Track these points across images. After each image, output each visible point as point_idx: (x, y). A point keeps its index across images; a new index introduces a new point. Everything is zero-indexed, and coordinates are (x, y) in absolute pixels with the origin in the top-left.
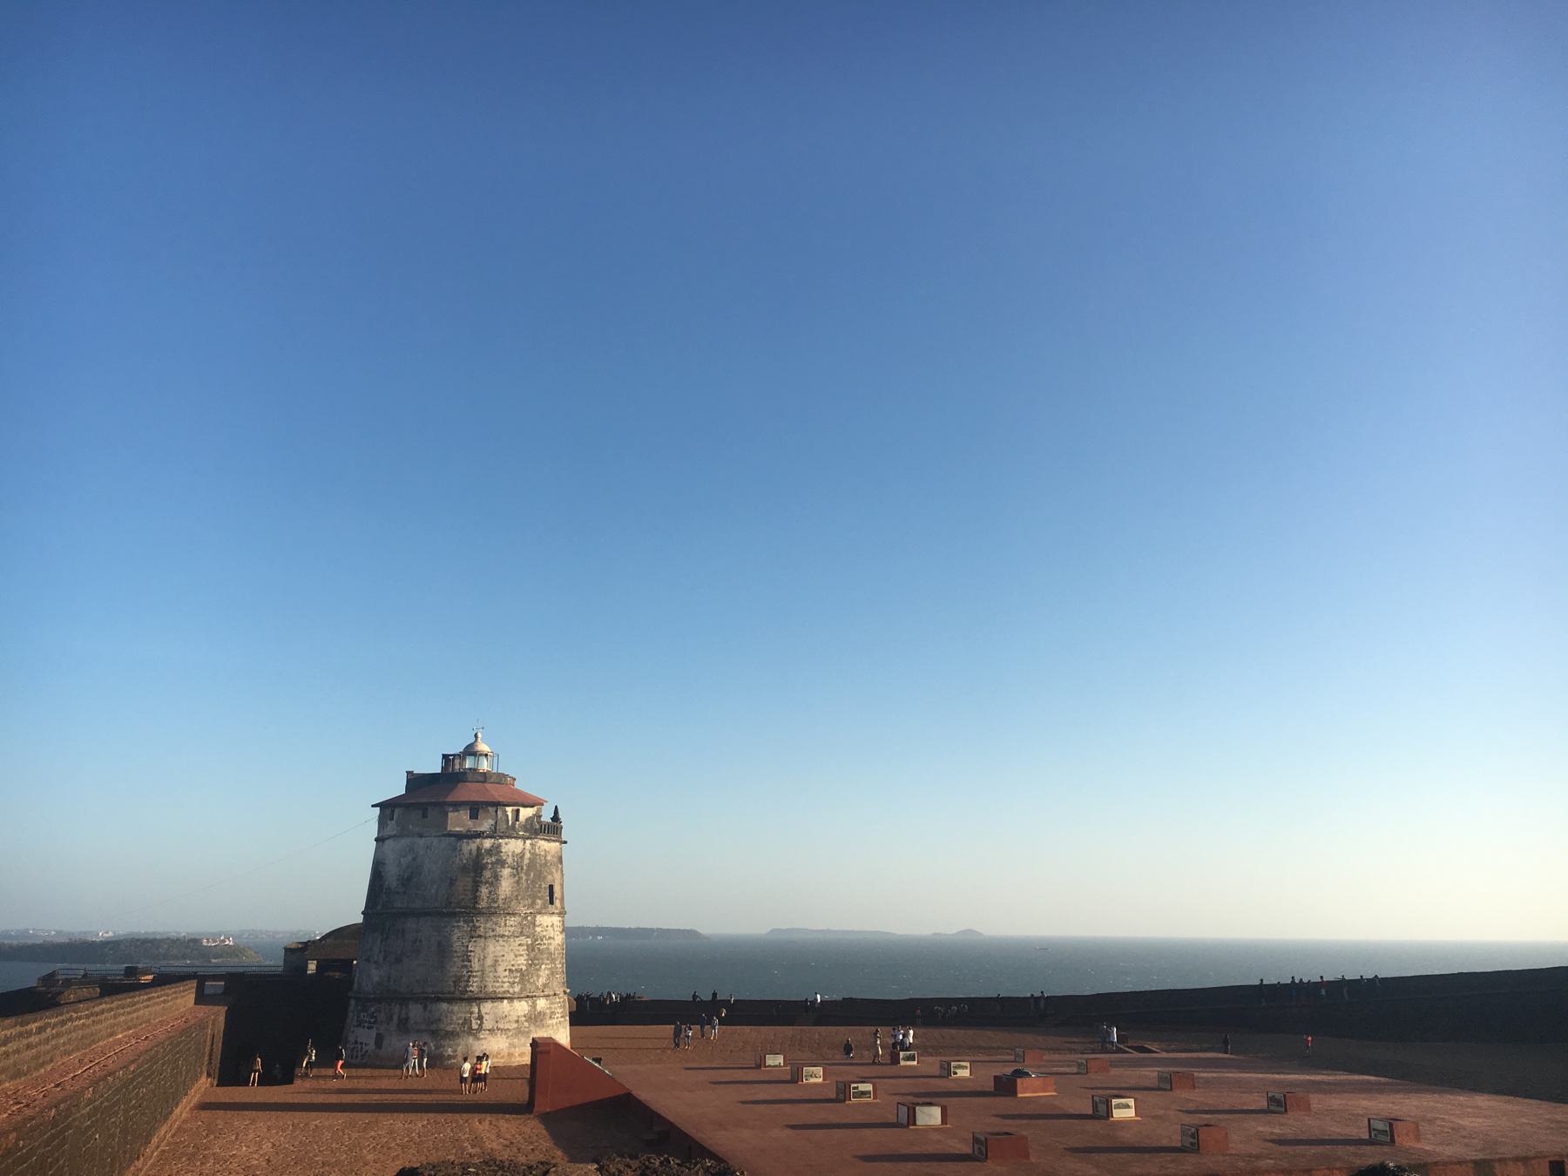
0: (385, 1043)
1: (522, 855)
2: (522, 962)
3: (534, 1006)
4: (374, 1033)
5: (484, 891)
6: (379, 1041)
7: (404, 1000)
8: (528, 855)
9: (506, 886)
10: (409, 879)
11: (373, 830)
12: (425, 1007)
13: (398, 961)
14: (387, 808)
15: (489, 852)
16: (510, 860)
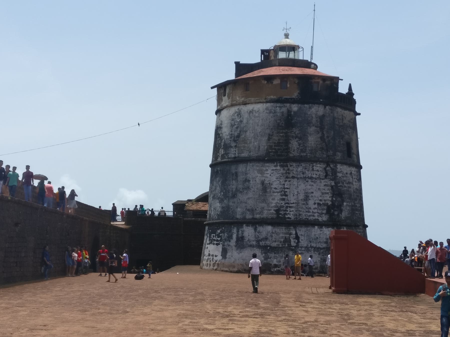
1: (322, 118)
2: (328, 198)
7: (240, 224)
9: (313, 140)
10: (238, 136)
12: (255, 229)
13: (234, 196)
16: (314, 120)
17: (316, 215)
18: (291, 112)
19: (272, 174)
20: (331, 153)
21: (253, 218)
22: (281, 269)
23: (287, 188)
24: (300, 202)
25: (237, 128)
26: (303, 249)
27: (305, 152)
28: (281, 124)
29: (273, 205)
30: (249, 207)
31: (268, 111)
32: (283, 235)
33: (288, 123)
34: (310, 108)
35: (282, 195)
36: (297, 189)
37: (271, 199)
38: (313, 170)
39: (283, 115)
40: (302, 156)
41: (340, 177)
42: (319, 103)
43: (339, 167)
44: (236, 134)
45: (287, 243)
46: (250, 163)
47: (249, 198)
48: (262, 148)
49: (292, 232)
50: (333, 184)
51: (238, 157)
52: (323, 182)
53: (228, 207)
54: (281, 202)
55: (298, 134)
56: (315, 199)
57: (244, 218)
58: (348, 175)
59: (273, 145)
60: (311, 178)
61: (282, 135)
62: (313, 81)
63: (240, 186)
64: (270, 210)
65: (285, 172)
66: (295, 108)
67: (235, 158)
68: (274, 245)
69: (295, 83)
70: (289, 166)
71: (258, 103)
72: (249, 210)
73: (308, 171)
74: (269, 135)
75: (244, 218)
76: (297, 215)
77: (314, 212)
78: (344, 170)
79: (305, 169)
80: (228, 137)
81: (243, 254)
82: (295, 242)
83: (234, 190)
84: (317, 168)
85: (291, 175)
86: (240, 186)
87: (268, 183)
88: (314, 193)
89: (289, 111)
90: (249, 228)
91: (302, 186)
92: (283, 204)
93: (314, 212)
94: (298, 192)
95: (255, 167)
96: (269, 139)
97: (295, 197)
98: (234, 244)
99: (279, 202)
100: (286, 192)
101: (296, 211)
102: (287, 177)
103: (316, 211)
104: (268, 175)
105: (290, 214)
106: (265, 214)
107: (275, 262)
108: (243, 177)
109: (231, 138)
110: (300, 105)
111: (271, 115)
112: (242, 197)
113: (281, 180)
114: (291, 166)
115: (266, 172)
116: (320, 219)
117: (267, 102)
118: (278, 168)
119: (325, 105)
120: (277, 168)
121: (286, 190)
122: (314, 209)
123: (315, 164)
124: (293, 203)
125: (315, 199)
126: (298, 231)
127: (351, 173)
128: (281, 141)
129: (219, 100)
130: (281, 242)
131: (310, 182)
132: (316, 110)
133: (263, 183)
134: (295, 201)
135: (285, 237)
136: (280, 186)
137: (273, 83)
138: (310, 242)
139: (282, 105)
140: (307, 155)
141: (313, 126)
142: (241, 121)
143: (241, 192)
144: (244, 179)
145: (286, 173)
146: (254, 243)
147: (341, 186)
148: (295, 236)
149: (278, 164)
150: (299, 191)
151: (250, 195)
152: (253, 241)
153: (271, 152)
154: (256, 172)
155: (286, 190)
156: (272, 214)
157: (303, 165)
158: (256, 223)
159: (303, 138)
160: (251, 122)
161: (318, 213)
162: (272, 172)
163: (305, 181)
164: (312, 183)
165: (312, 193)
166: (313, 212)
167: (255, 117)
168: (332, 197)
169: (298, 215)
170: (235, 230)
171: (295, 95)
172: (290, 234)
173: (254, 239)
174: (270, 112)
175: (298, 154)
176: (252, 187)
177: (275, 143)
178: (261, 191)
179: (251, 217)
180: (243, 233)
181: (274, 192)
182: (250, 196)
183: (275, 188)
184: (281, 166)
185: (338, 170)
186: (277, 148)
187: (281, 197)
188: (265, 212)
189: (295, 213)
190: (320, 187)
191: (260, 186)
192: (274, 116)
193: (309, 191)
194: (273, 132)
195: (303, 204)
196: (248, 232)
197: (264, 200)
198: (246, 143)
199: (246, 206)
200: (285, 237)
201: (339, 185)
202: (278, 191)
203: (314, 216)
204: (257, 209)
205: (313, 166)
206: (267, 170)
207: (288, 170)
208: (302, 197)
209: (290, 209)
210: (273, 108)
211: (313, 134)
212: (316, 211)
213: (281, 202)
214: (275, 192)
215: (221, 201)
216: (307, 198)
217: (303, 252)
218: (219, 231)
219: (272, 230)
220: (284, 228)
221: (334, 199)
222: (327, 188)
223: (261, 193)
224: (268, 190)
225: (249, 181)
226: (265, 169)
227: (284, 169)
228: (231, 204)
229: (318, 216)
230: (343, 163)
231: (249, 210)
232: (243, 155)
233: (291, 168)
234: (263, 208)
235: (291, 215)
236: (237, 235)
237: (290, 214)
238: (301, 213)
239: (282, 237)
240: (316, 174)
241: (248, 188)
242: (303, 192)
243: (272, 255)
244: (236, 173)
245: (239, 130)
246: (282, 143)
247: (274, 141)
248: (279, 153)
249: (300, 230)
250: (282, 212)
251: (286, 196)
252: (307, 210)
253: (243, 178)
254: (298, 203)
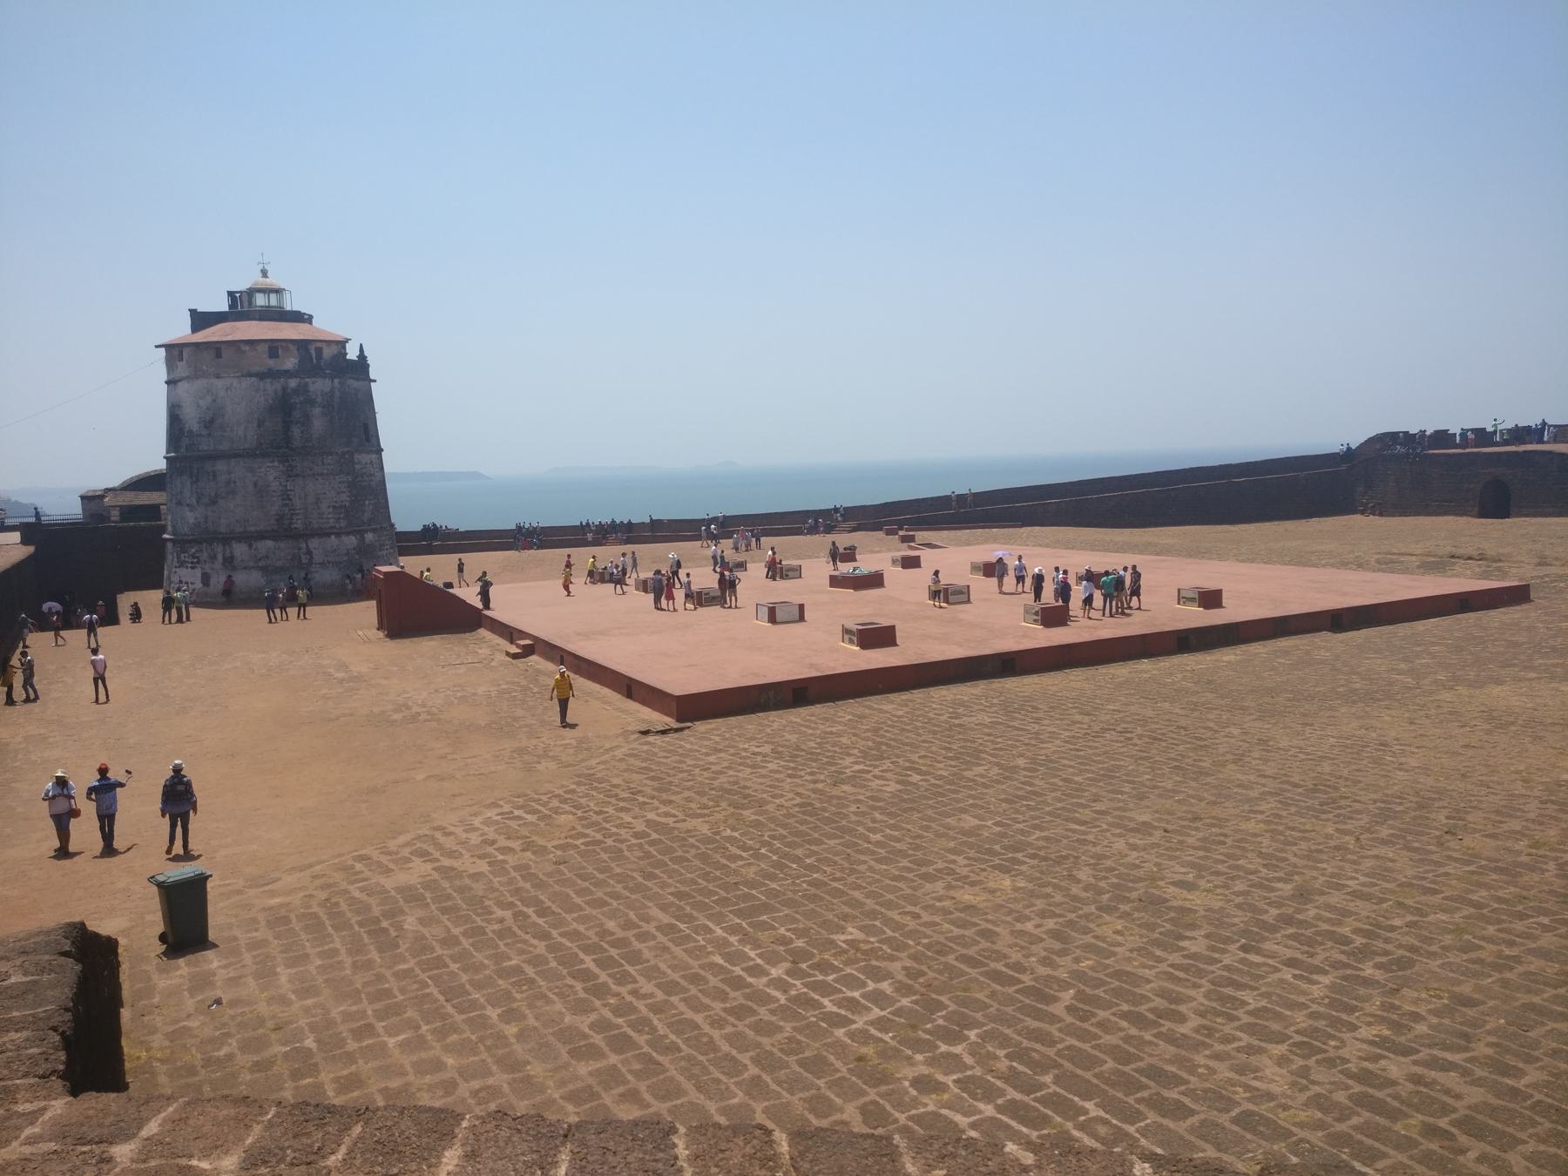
3: (363, 539)
4: (198, 573)
5: (296, 431)
6: (206, 579)
7: (226, 540)
8: (337, 394)
9: (318, 424)
10: (212, 421)
11: (162, 373)
12: (250, 546)
13: (214, 502)
14: (174, 351)
15: (296, 391)
16: (319, 400)
129: (170, 364)
132: (319, 386)
133: (255, 484)
196: (239, 550)
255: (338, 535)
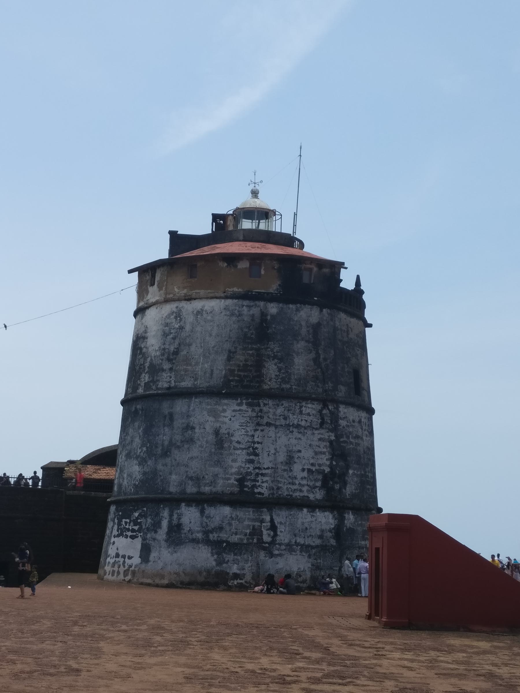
0: (153, 555)
1: (316, 328)
4: (138, 543)
6: (146, 552)
7: (175, 501)
13: (166, 453)
17: (305, 489)
18: (267, 315)
19: (233, 417)
20: (329, 385)
21: (199, 493)
22: (246, 582)
23: (258, 443)
24: (279, 466)
25: (174, 338)
26: (283, 547)
27: (288, 382)
28: (249, 335)
29: (234, 470)
30: (191, 474)
31: (228, 313)
32: (250, 523)
33: (260, 333)
34: (297, 310)
35: (248, 454)
36: (275, 445)
37: (230, 461)
38: (301, 413)
39: (253, 320)
40: (283, 389)
41: (344, 427)
42: (313, 304)
43: (342, 409)
44: (172, 349)
45: (256, 537)
46: (196, 398)
47: (192, 458)
48: (216, 372)
49: (264, 517)
50: (333, 438)
51: (175, 387)
52: (318, 434)
53: (155, 473)
54: (247, 466)
55: (277, 352)
56: (304, 461)
57: (183, 492)
58: (356, 424)
59: (236, 369)
60: (298, 426)
61: (251, 352)
62: (303, 266)
63: (178, 438)
64: (229, 479)
65: (254, 414)
66: (273, 309)
67: (169, 388)
68: (235, 539)
69: (273, 268)
70: (262, 405)
71: (212, 298)
72: (191, 478)
73: (294, 414)
74: (230, 351)
75: (183, 492)
76: (273, 489)
77: (301, 483)
78: (348, 413)
79: (289, 410)
80: (158, 353)
81: (179, 554)
82: (269, 535)
83: (166, 443)
84: (308, 411)
85: (265, 420)
86: (178, 438)
87: (226, 432)
88: (303, 451)
89: (263, 314)
90: (190, 509)
91: (283, 440)
92: (251, 468)
93: (301, 483)
94: (276, 449)
95: (204, 405)
96: (229, 359)
97: (271, 458)
98: (164, 537)
99: (243, 465)
100: (257, 448)
101: (272, 482)
102: (258, 424)
103: (304, 482)
104: (227, 420)
105: (262, 487)
106: (220, 486)
107: (235, 569)
108: (183, 421)
109: (163, 355)
110: (281, 305)
111: (234, 318)
112: (179, 456)
113: (248, 429)
114: (265, 405)
115: (222, 414)
116: (311, 496)
117: (226, 298)
118: (244, 407)
119: (321, 306)
120: (241, 408)
121: (256, 445)
122: (302, 478)
123: (304, 404)
124: (268, 468)
125: (304, 461)
126: (274, 517)
127: (360, 422)
128: (249, 363)
130: (246, 535)
131: (296, 434)
132: (308, 315)
133: (217, 432)
134: (270, 465)
135: (254, 526)
136: (247, 439)
137: (236, 266)
138: (295, 535)
139: (252, 304)
140: (291, 388)
141: (302, 339)
142: (181, 328)
143: (178, 447)
144: (185, 425)
145: (257, 417)
146: (200, 536)
147: (345, 442)
148: (269, 524)
149: (244, 401)
150: (278, 447)
151: (195, 451)
152: (198, 532)
153: (232, 380)
154: (205, 413)
155: (256, 445)
156: (232, 485)
157: (286, 403)
158: (201, 501)
159: (285, 358)
160: (199, 329)
161: (308, 485)
162: (234, 414)
163: (288, 432)
164: (300, 436)
165: (300, 451)
166: (300, 484)
167: (206, 321)
168: (331, 459)
169: (275, 488)
170: (166, 513)
171: (274, 287)
172: (262, 521)
173: (199, 529)
174: (232, 314)
175: (278, 386)
176: (199, 440)
177: (239, 366)
178: (213, 446)
179: (195, 490)
180: (180, 519)
181: (235, 449)
182: (195, 455)
183: (239, 442)
184: (249, 405)
185: (341, 415)
186: (242, 374)
187: (248, 458)
188: (221, 482)
189: (271, 485)
190: (312, 443)
191: (211, 438)
192: (238, 321)
193: (293, 449)
194: (236, 348)
195: (285, 470)
197: (218, 461)
198: (191, 365)
199: (187, 472)
200: (254, 526)
201: (342, 440)
202: (243, 447)
203: (301, 491)
204: (206, 477)
205: (301, 407)
206: (224, 411)
207: (261, 411)
208: (282, 457)
209: (263, 478)
210: (237, 308)
211: (302, 353)
212: (304, 482)
213: (247, 466)
214: (237, 449)
215: (142, 462)
216: (290, 461)
217: (283, 552)
218: (136, 514)
219: (231, 514)
220: (251, 510)
221: (334, 463)
222: (323, 444)
223: (213, 450)
224: (226, 445)
225: (193, 428)
226: (220, 408)
227: (253, 410)
228: (160, 467)
229: (308, 491)
230: (348, 404)
231: (191, 478)
232: (183, 384)
233: (265, 409)
234: (217, 475)
235: (265, 489)
236: (170, 522)
237: (262, 487)
238: (280, 485)
239: (249, 526)
240: (306, 421)
241: (191, 441)
242: (285, 450)
243: (230, 557)
244: (171, 416)
245: (177, 342)
246: (251, 366)
247: (238, 362)
248: (245, 383)
249: (278, 515)
250: (248, 484)
251: (257, 455)
252: (291, 481)
253: (183, 423)
254: (275, 469)
255: (312, 506)
